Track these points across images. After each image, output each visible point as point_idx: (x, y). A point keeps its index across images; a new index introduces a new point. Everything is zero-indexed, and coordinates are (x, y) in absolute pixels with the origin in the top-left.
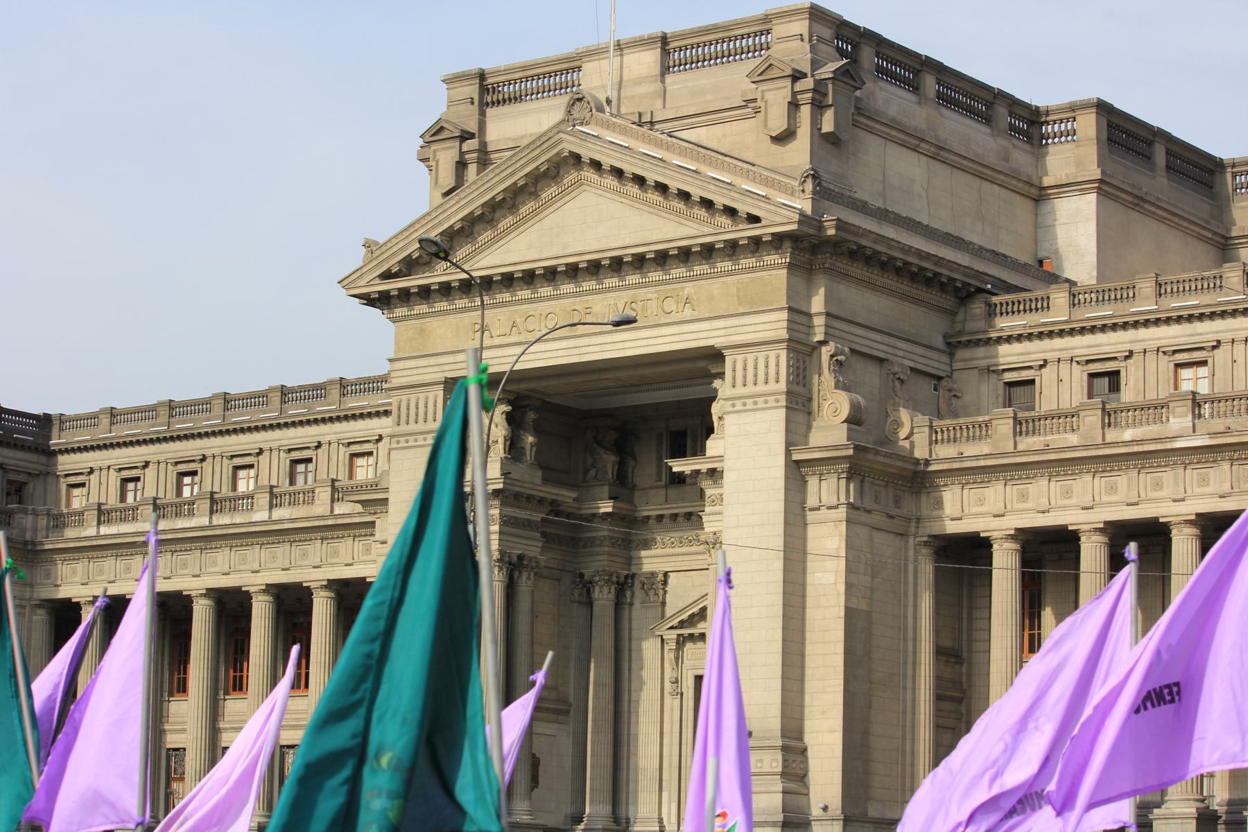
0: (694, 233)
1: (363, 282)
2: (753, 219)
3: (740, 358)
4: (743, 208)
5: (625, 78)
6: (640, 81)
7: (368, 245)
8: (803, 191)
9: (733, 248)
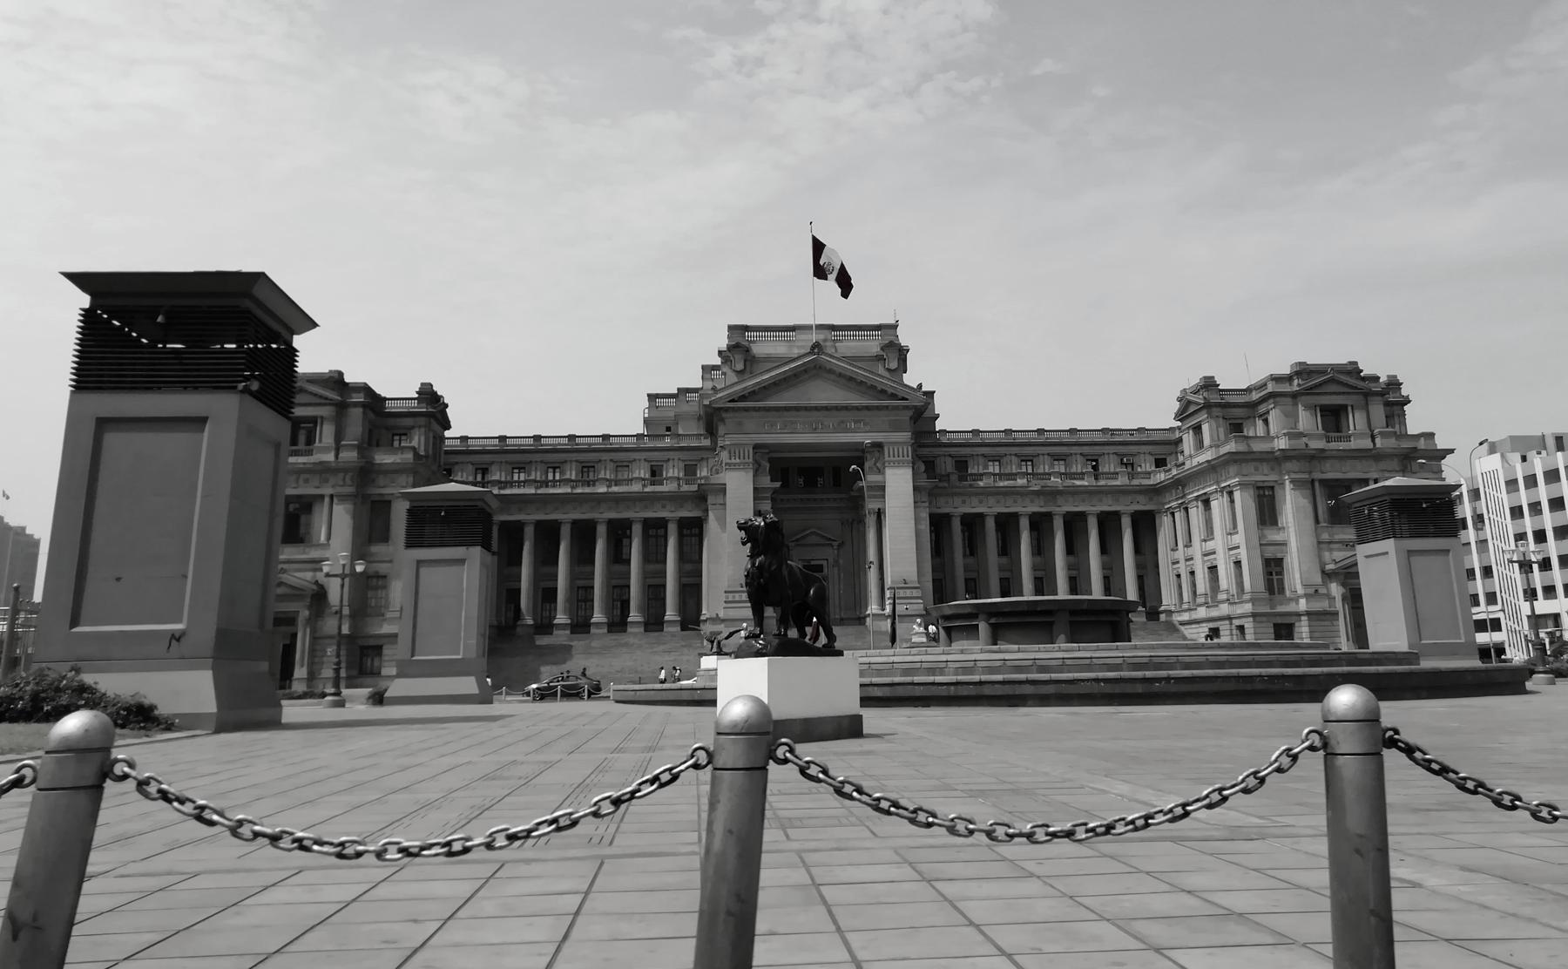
9: (896, 408)
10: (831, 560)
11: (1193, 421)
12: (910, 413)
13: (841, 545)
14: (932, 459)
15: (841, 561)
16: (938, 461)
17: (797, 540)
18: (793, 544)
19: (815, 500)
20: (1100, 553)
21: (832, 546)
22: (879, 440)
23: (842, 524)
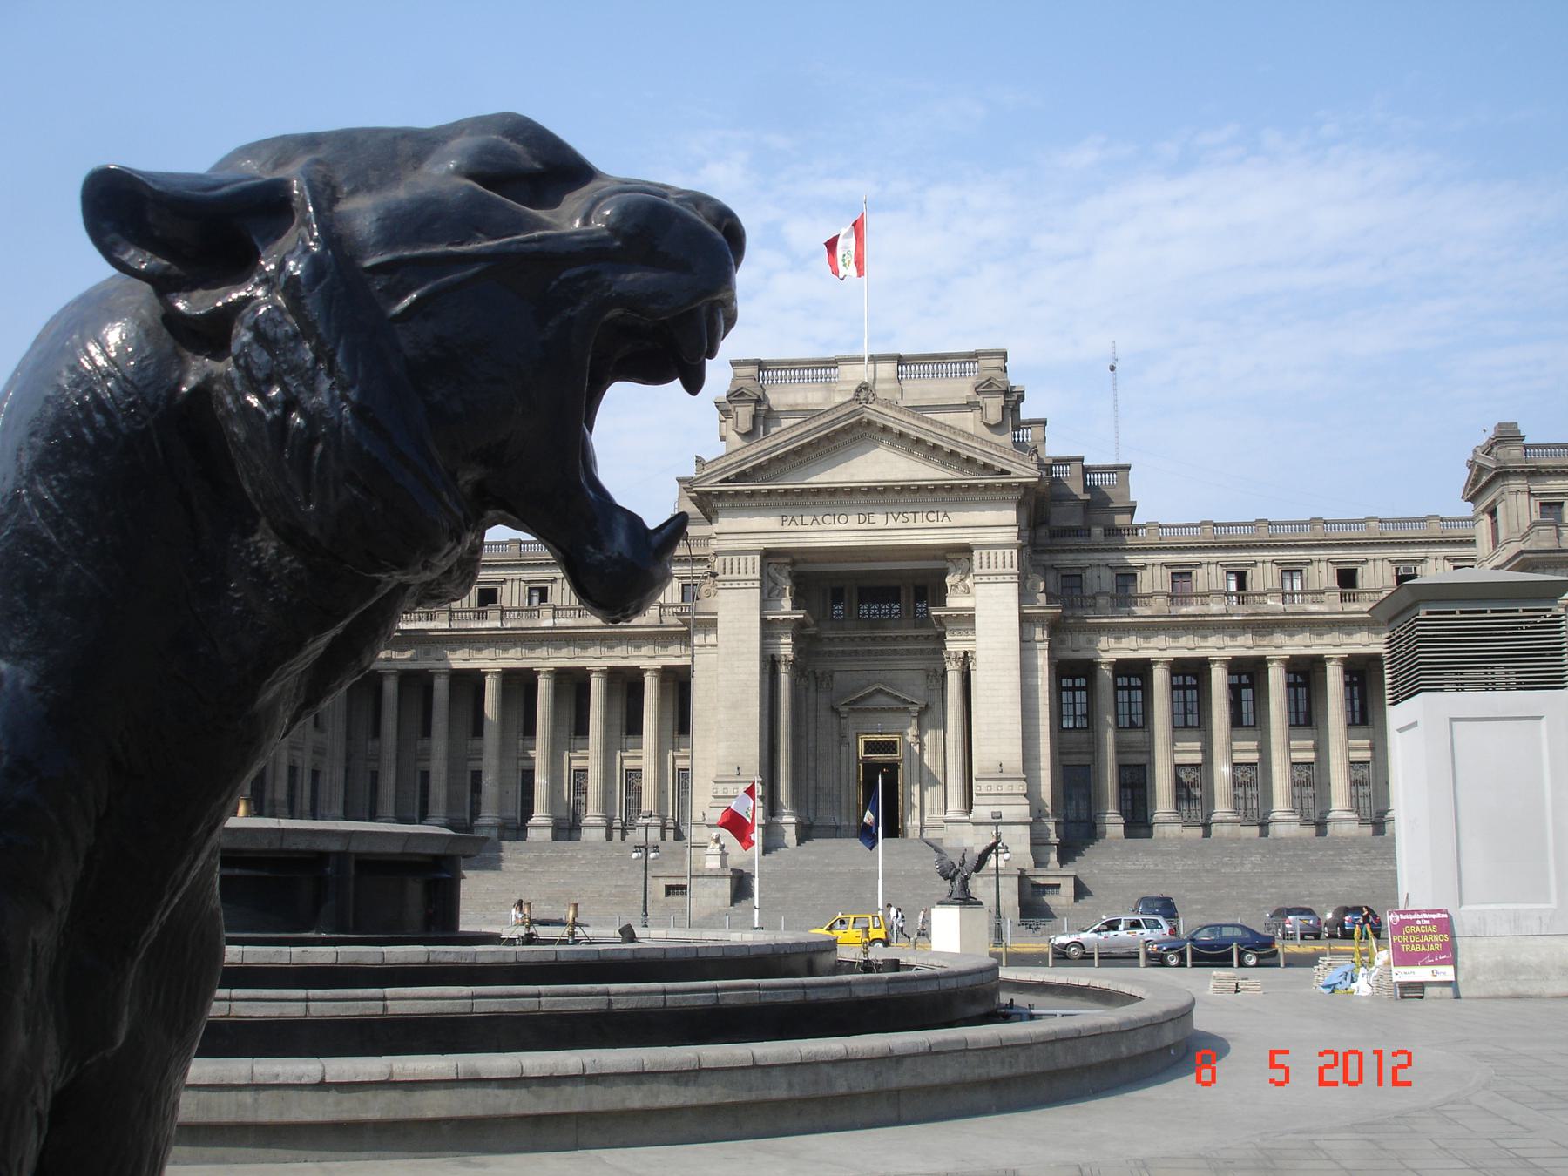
0: (951, 477)
1: (707, 483)
2: (1003, 472)
3: (984, 552)
4: (998, 465)
5: (878, 376)
6: (884, 381)
7: (699, 460)
8: (1031, 460)
11: (1486, 501)
12: (1017, 496)
14: (1078, 572)
16: (1088, 574)
17: (854, 702)
18: (846, 709)
20: (1286, 725)
21: (910, 712)
23: (928, 676)
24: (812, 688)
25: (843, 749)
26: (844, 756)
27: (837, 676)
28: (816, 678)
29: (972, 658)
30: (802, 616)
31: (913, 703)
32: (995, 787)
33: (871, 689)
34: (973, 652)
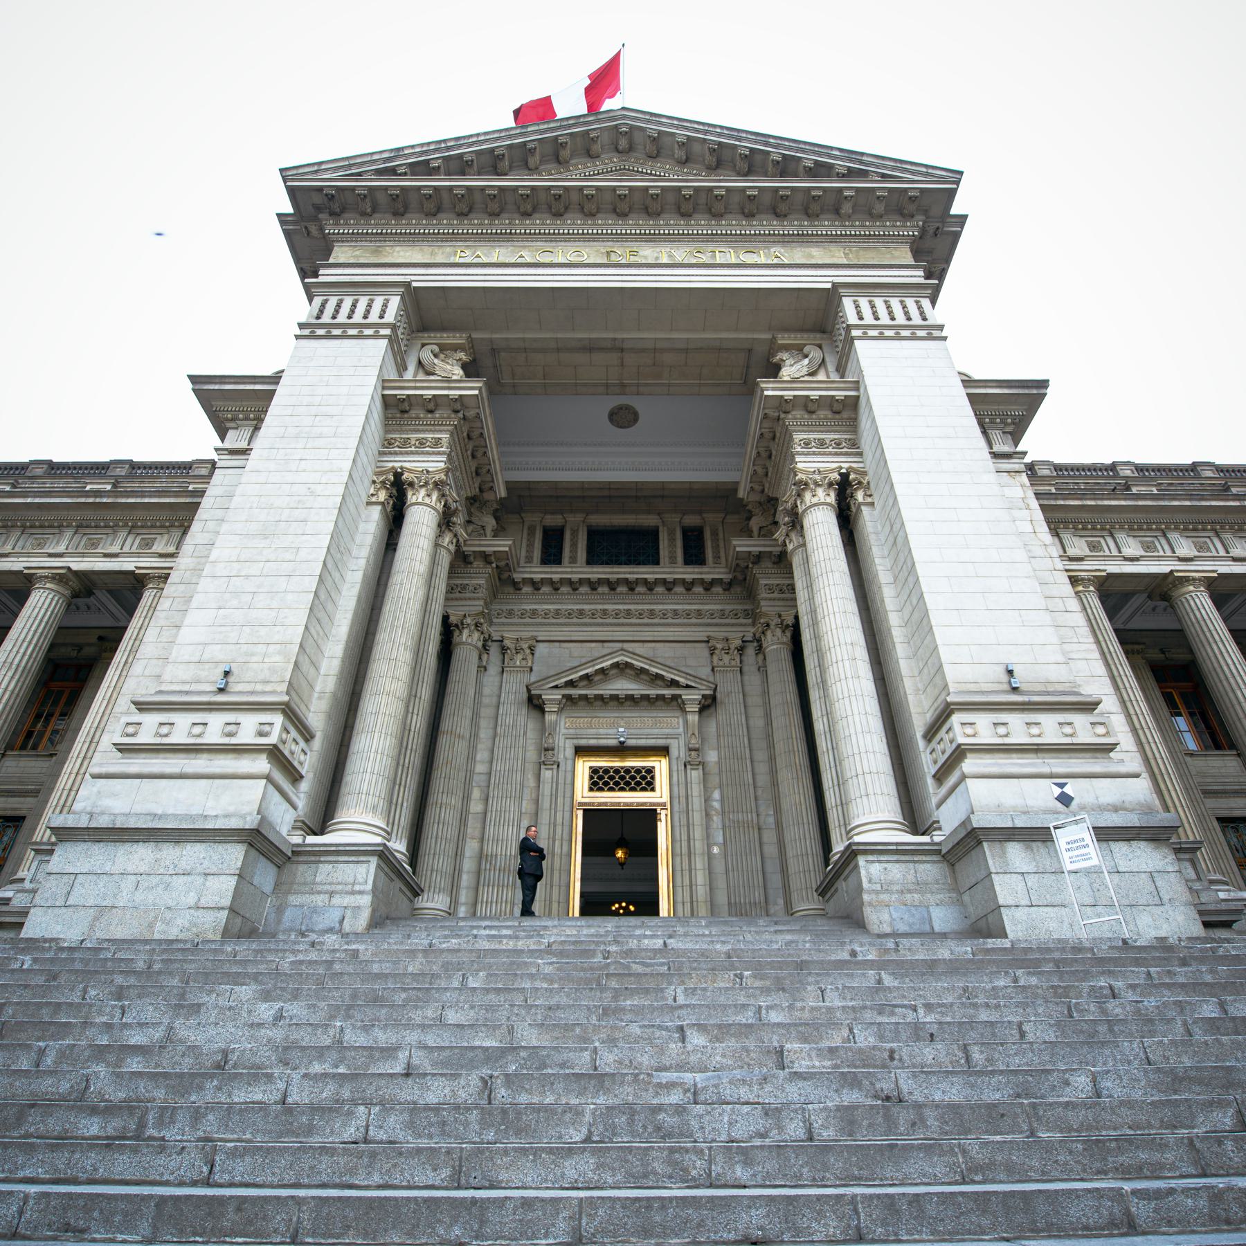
10: (677, 749)
13: (709, 704)
15: (712, 756)
17: (571, 684)
19: (631, 585)
22: (829, 286)
23: (712, 651)
24: (493, 669)
25: (547, 774)
26: (546, 789)
27: (541, 649)
28: (504, 650)
29: (860, 483)
30: (476, 392)
31: (688, 686)
32: (1018, 728)
33: (607, 664)
34: (856, 471)
